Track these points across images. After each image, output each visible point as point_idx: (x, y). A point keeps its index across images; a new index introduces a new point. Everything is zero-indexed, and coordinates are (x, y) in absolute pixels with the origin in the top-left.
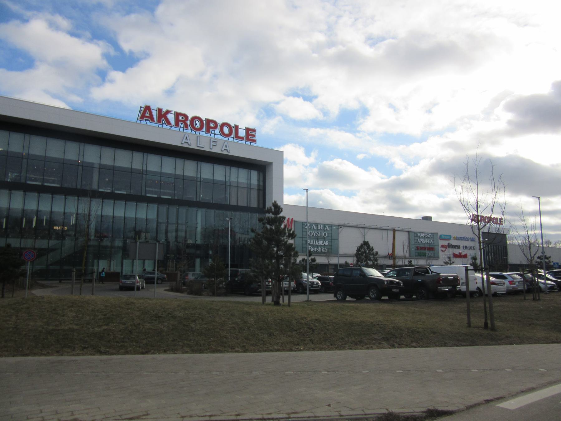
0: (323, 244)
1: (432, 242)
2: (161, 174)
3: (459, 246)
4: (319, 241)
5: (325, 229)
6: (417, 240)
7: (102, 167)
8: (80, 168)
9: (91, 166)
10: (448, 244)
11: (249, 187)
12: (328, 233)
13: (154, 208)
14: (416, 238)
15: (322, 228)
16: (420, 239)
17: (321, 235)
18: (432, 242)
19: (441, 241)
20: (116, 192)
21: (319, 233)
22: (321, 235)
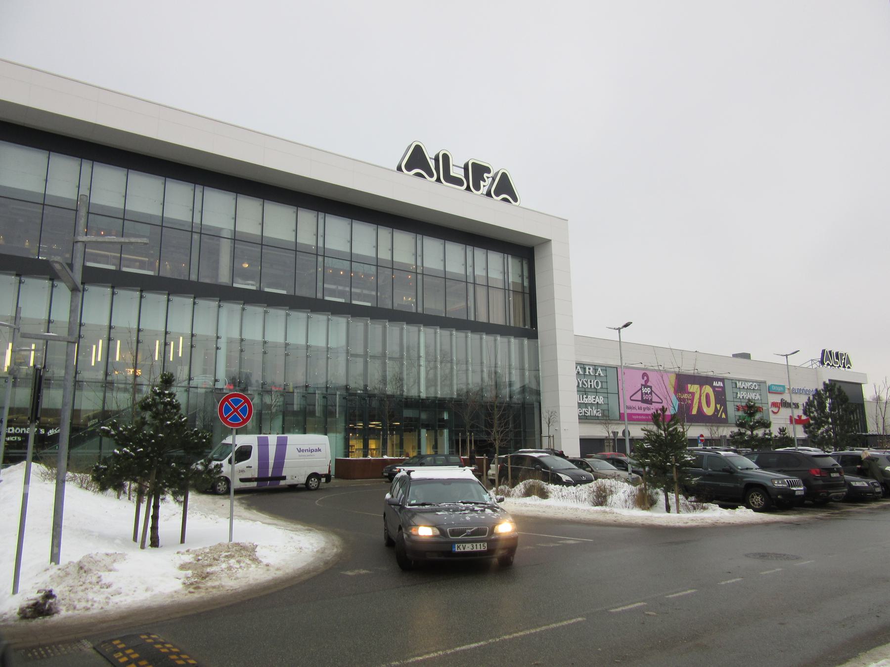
0: (594, 401)
1: (759, 397)
2: (351, 258)
3: (797, 404)
4: (589, 396)
5: (597, 374)
6: (737, 394)
7: (236, 238)
8: (196, 237)
9: (215, 235)
10: (782, 400)
11: (507, 288)
12: (602, 382)
13: (341, 323)
14: (735, 390)
15: (592, 374)
16: (741, 393)
17: (591, 385)
18: (758, 397)
19: (773, 395)
20: (267, 290)
21: (587, 382)
22: (591, 385)
